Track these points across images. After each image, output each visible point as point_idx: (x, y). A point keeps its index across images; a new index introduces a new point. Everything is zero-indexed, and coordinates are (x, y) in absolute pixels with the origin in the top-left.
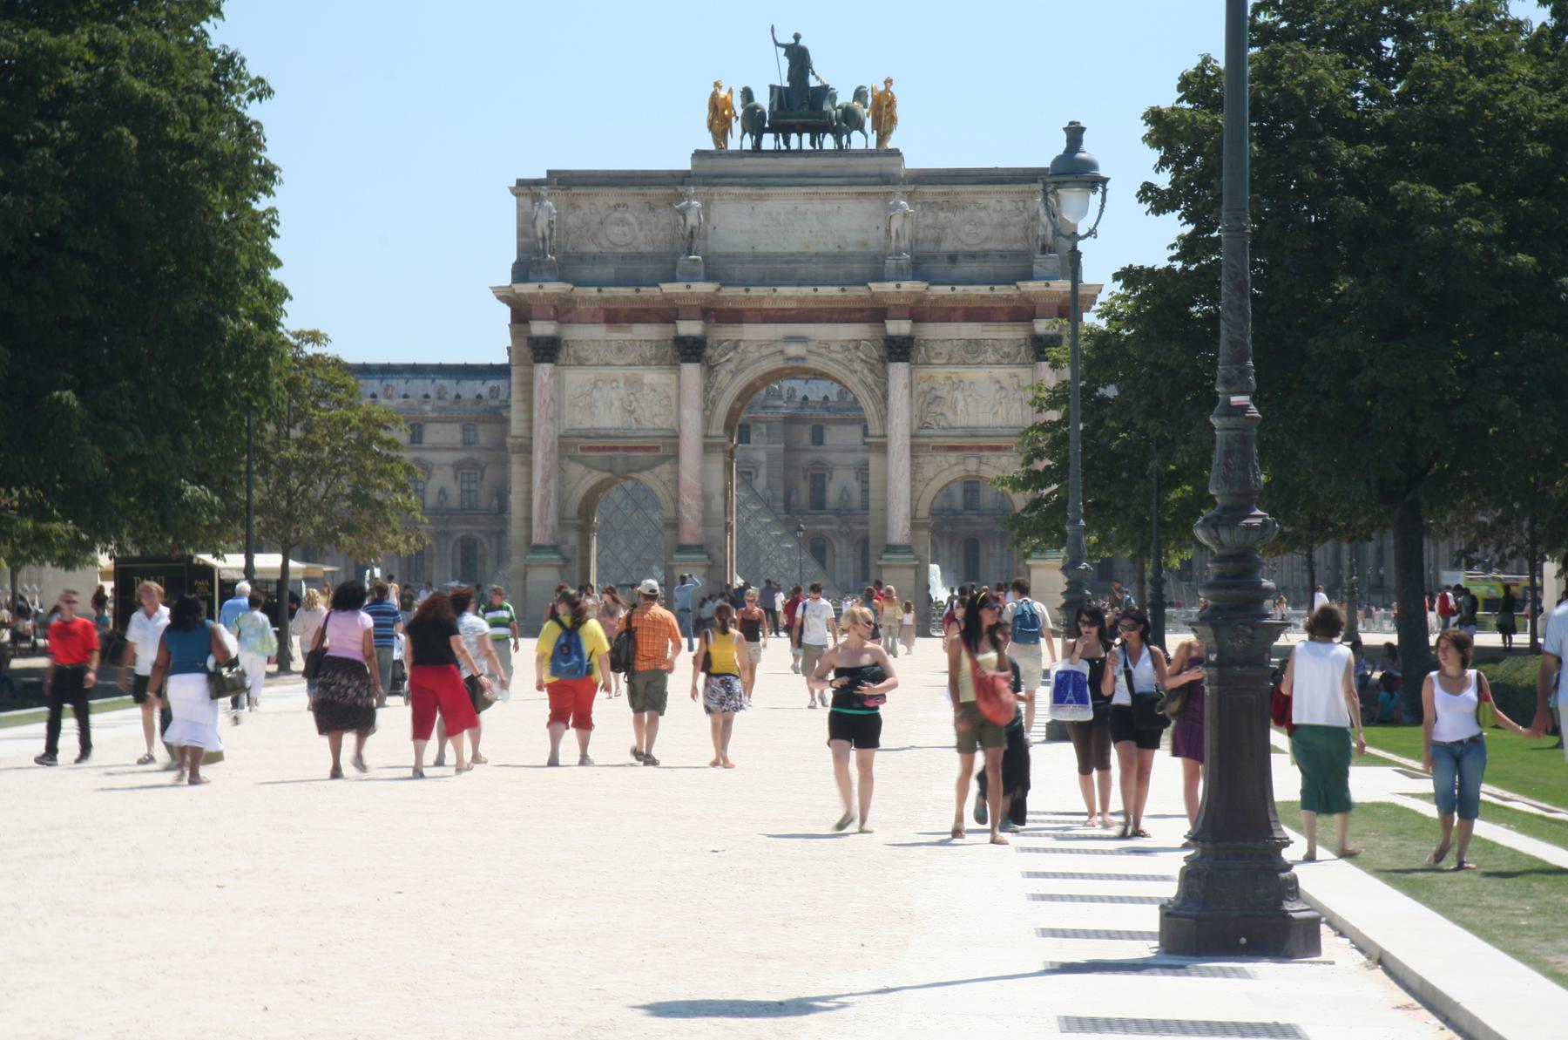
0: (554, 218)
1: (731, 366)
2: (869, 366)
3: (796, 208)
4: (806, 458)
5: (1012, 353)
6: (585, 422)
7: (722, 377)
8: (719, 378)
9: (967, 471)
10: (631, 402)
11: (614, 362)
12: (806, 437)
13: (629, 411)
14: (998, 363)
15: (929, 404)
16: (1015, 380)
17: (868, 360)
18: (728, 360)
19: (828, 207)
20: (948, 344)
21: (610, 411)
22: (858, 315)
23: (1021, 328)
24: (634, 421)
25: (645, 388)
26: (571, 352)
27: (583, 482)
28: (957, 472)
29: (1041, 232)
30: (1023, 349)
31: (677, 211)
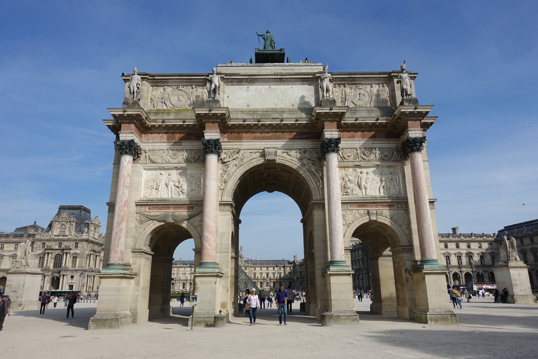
0: (140, 83)
1: (235, 162)
2: (312, 162)
3: (270, 87)
4: (253, 272)
5: (390, 156)
6: (154, 195)
7: (232, 168)
8: (229, 169)
9: (370, 220)
10: (179, 182)
11: (171, 160)
12: (253, 269)
13: (178, 187)
15: (346, 182)
16: (392, 169)
17: (311, 159)
18: (234, 159)
19: (286, 87)
20: (355, 150)
21: (168, 188)
22: (305, 136)
23: (393, 142)
24: (180, 193)
25: (188, 176)
26: (147, 155)
27: (149, 227)
28: (366, 219)
29: (405, 87)
30: (395, 153)
31: (208, 80)
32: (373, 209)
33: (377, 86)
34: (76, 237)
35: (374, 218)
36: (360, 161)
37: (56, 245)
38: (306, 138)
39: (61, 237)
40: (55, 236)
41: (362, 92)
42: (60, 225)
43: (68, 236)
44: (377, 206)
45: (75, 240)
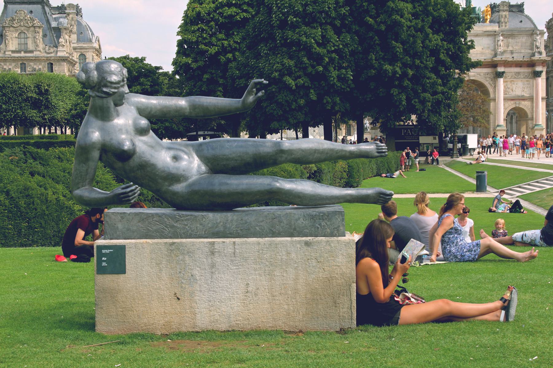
14: (524, 78)
19: (479, 38)
28: (514, 106)
29: (537, 44)
32: (517, 102)
33: (526, 38)
34: (49, 53)
35: (517, 106)
36: (514, 78)
37: (16, 66)
38: (488, 67)
39: (23, 54)
40: (13, 52)
41: (518, 40)
42: (17, 34)
43: (34, 52)
44: (519, 100)
45: (48, 59)
